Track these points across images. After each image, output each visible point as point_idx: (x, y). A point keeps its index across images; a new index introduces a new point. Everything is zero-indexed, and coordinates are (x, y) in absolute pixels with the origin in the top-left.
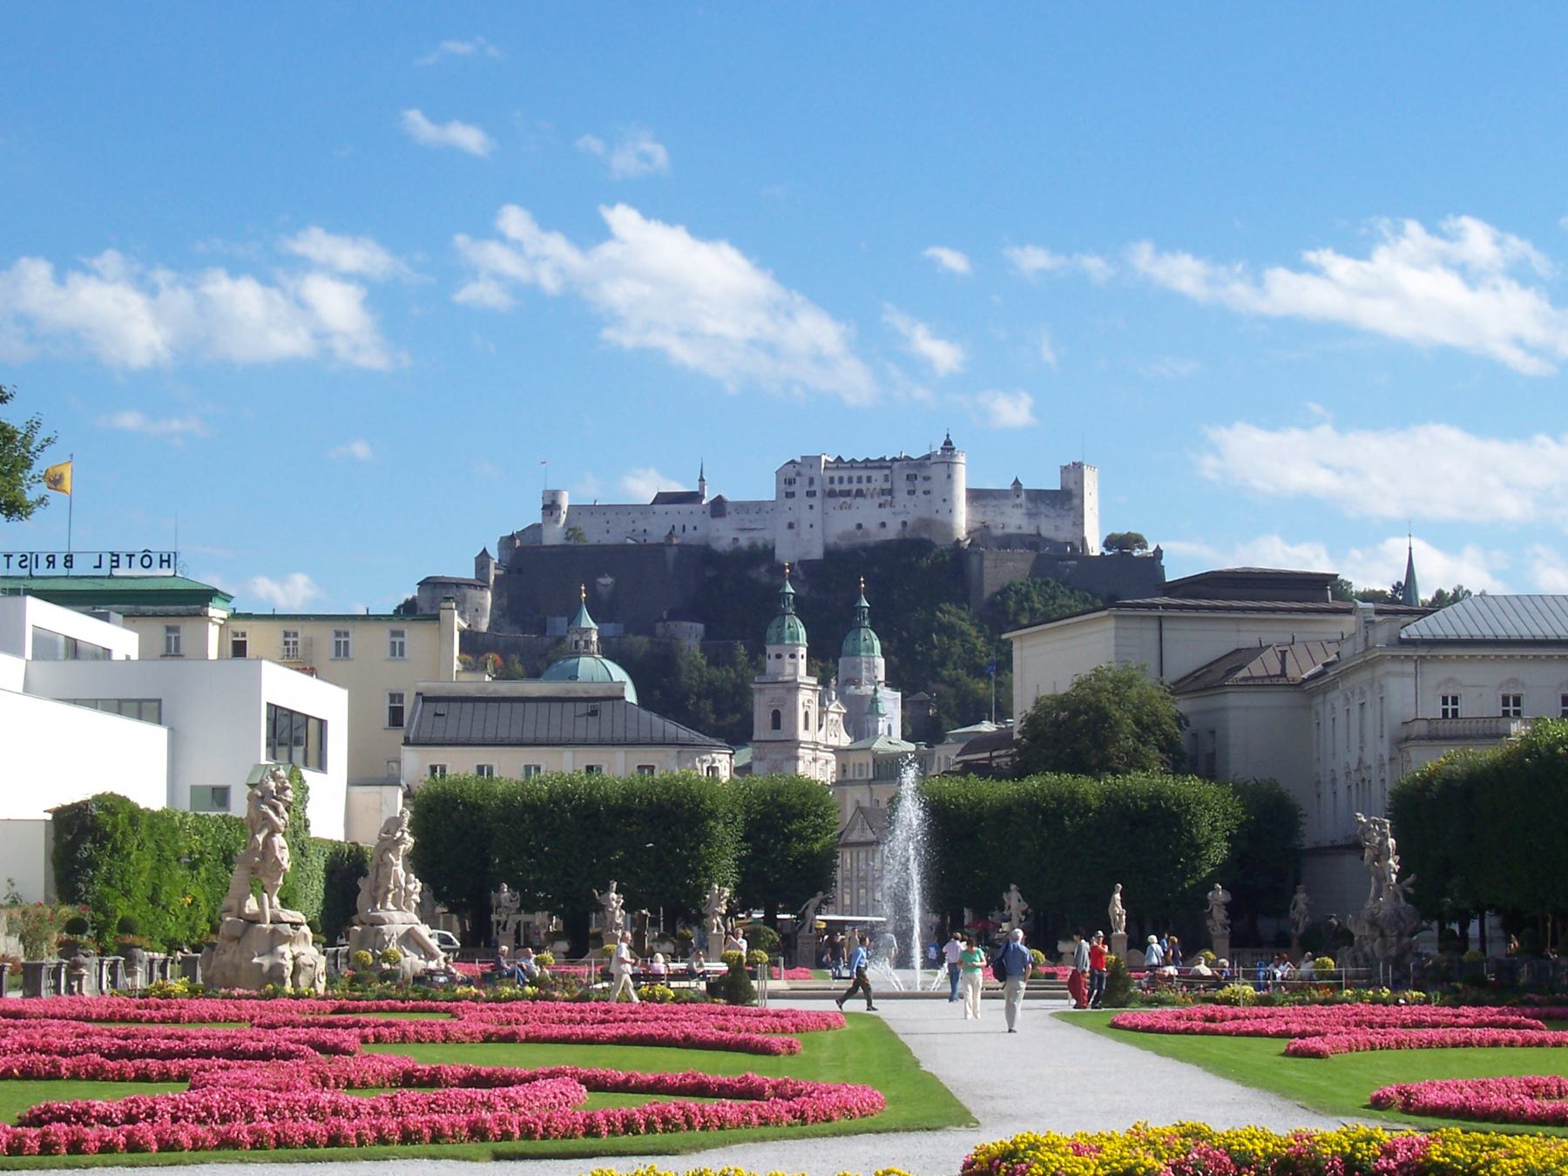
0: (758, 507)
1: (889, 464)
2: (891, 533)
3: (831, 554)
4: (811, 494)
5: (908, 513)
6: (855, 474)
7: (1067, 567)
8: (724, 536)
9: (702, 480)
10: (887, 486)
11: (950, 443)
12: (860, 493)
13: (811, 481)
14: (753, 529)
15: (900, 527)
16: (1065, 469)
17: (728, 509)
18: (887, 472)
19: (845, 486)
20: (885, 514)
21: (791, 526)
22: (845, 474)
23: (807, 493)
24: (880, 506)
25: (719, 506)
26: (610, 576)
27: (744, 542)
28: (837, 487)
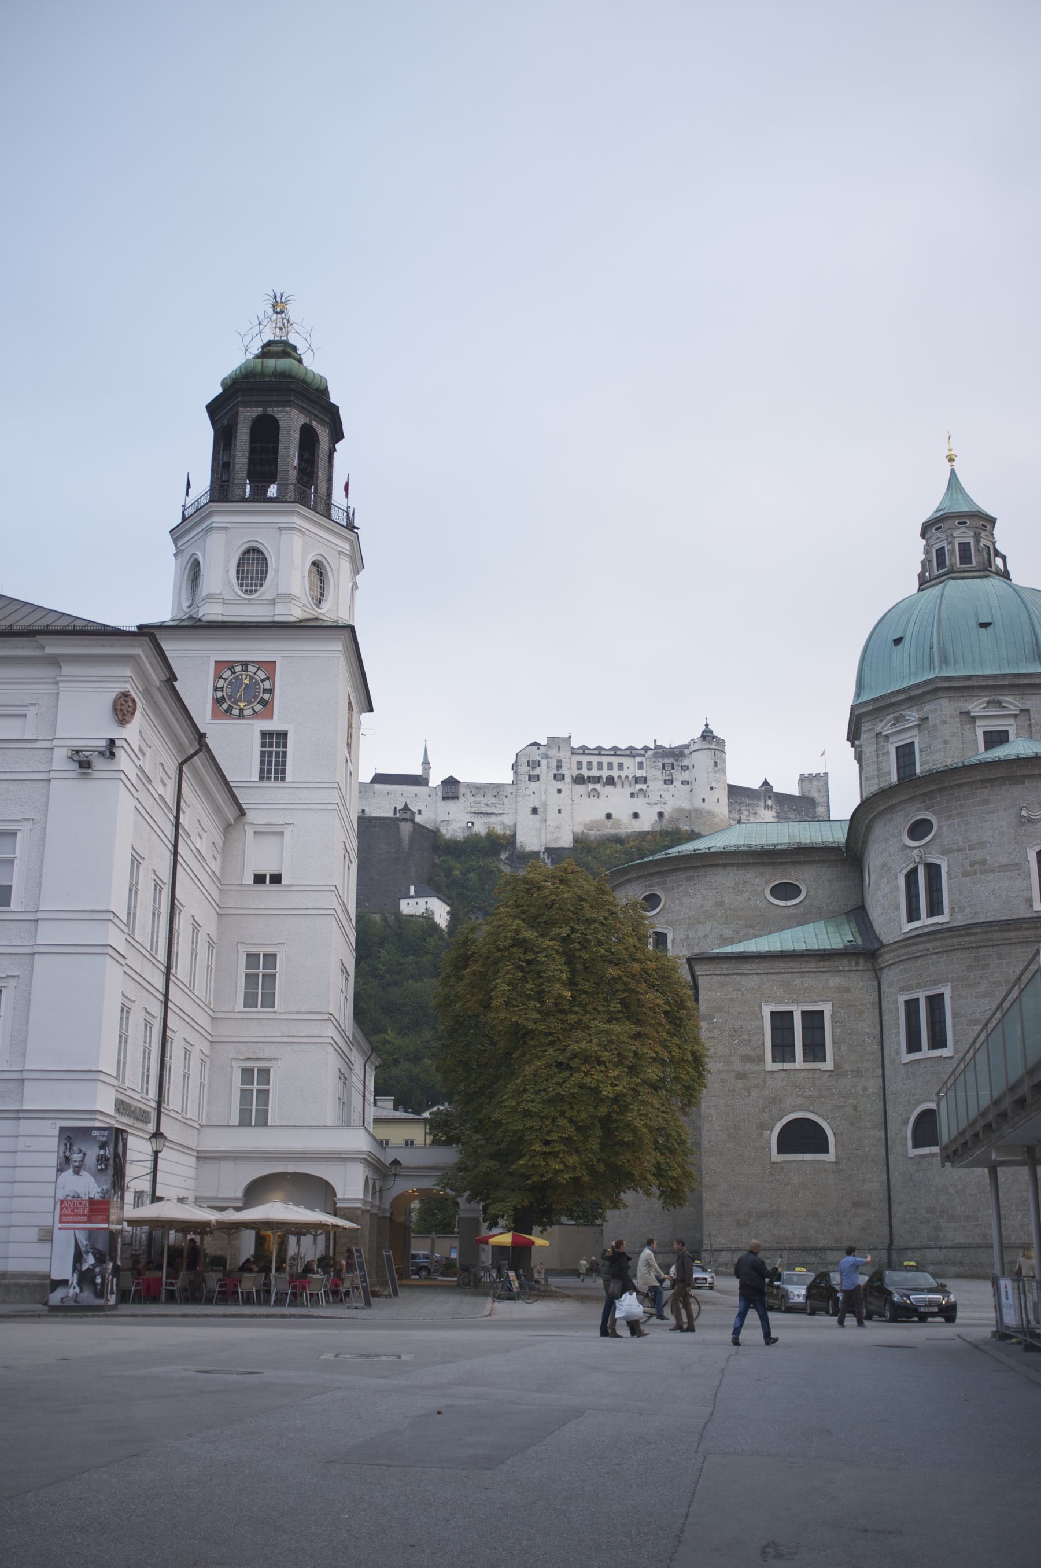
1: (643, 752)
2: (647, 823)
3: (579, 840)
4: (559, 777)
5: (666, 803)
6: (605, 760)
9: (426, 763)
10: (639, 773)
12: (610, 781)
13: (559, 767)
15: (655, 817)
16: (803, 779)
18: (638, 759)
19: (594, 773)
21: (535, 811)
22: (595, 760)
23: (555, 775)
24: (632, 795)
27: (480, 828)
28: (585, 773)
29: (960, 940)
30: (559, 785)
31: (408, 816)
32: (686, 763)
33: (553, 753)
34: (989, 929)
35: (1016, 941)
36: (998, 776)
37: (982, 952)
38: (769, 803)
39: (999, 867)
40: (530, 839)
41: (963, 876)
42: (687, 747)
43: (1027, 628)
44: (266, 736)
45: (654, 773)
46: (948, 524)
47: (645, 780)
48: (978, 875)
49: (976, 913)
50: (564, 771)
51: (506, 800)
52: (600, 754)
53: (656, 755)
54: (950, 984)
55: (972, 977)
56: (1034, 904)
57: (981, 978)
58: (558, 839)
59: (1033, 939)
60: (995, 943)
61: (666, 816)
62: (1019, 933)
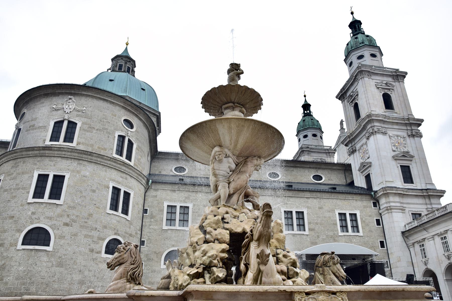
29: (12, 155)
34: (22, 150)
35: (31, 155)
36: (49, 92)
37: (19, 160)
39: (39, 127)
41: (26, 131)
43: (125, 83)
46: (118, 58)
48: (30, 131)
49: (24, 146)
54: (4, 175)
55: (12, 171)
56: (46, 142)
57: (14, 172)
59: (38, 155)
60: (24, 156)
62: (33, 152)
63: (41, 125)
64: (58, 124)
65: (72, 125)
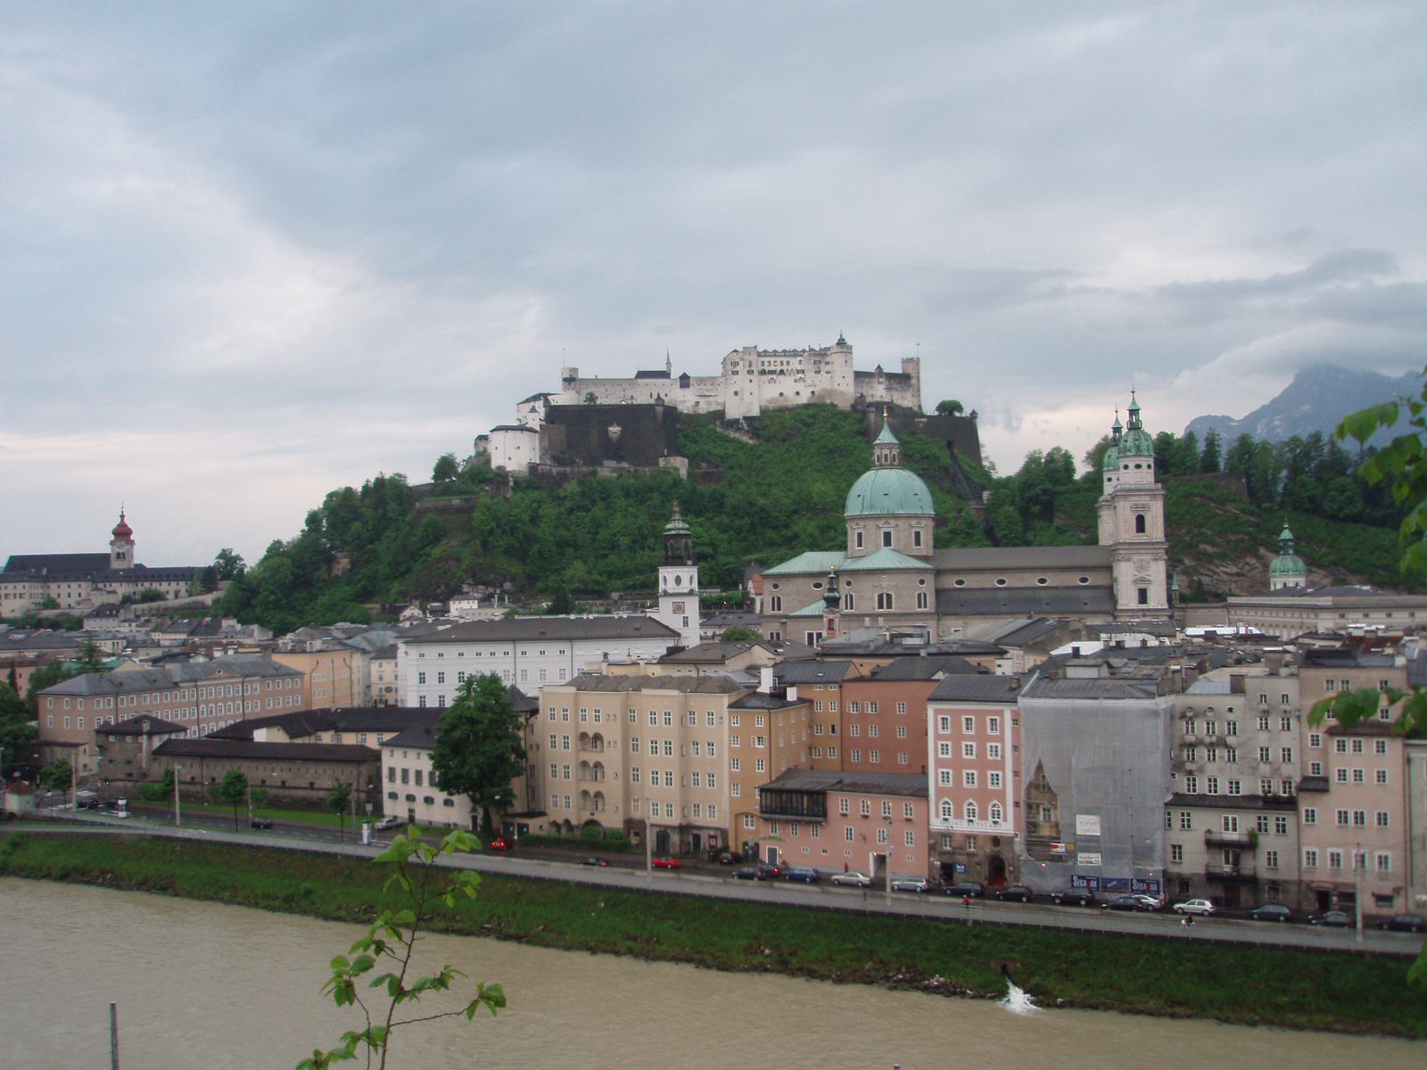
0: (712, 380)
2: (804, 398)
3: (764, 411)
4: (750, 372)
6: (779, 359)
7: (921, 422)
8: (685, 401)
9: (669, 363)
11: (844, 340)
12: (782, 372)
13: (750, 365)
14: (709, 396)
15: (810, 394)
17: (691, 382)
18: (799, 358)
19: (772, 368)
20: (800, 387)
21: (736, 393)
22: (772, 359)
24: (795, 381)
25: (685, 381)
26: (618, 425)
27: (704, 408)
28: (767, 368)
30: (751, 377)
31: (660, 402)
32: (828, 359)
33: (747, 357)
38: (881, 380)
40: (734, 412)
42: (828, 349)
44: (684, 618)
45: (808, 366)
47: (803, 372)
50: (753, 368)
51: (718, 387)
52: (775, 356)
53: (810, 355)
58: (750, 411)
61: (816, 393)
63: (868, 597)
64: (880, 597)
65: (889, 596)
